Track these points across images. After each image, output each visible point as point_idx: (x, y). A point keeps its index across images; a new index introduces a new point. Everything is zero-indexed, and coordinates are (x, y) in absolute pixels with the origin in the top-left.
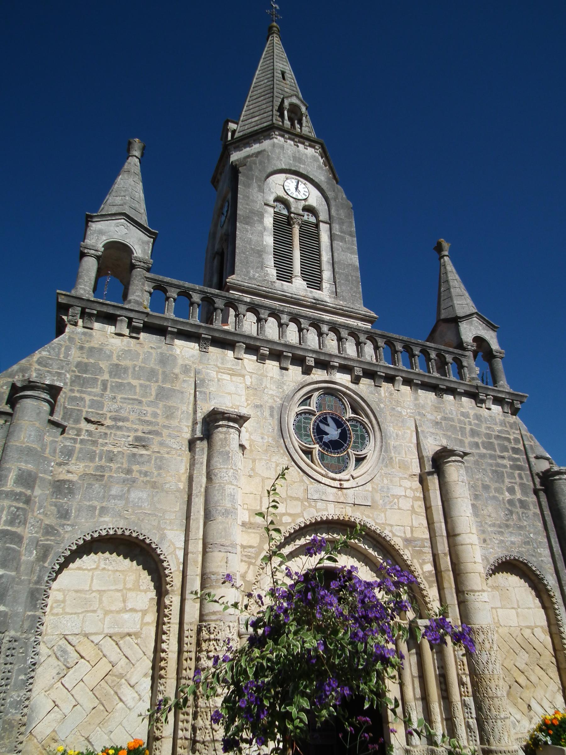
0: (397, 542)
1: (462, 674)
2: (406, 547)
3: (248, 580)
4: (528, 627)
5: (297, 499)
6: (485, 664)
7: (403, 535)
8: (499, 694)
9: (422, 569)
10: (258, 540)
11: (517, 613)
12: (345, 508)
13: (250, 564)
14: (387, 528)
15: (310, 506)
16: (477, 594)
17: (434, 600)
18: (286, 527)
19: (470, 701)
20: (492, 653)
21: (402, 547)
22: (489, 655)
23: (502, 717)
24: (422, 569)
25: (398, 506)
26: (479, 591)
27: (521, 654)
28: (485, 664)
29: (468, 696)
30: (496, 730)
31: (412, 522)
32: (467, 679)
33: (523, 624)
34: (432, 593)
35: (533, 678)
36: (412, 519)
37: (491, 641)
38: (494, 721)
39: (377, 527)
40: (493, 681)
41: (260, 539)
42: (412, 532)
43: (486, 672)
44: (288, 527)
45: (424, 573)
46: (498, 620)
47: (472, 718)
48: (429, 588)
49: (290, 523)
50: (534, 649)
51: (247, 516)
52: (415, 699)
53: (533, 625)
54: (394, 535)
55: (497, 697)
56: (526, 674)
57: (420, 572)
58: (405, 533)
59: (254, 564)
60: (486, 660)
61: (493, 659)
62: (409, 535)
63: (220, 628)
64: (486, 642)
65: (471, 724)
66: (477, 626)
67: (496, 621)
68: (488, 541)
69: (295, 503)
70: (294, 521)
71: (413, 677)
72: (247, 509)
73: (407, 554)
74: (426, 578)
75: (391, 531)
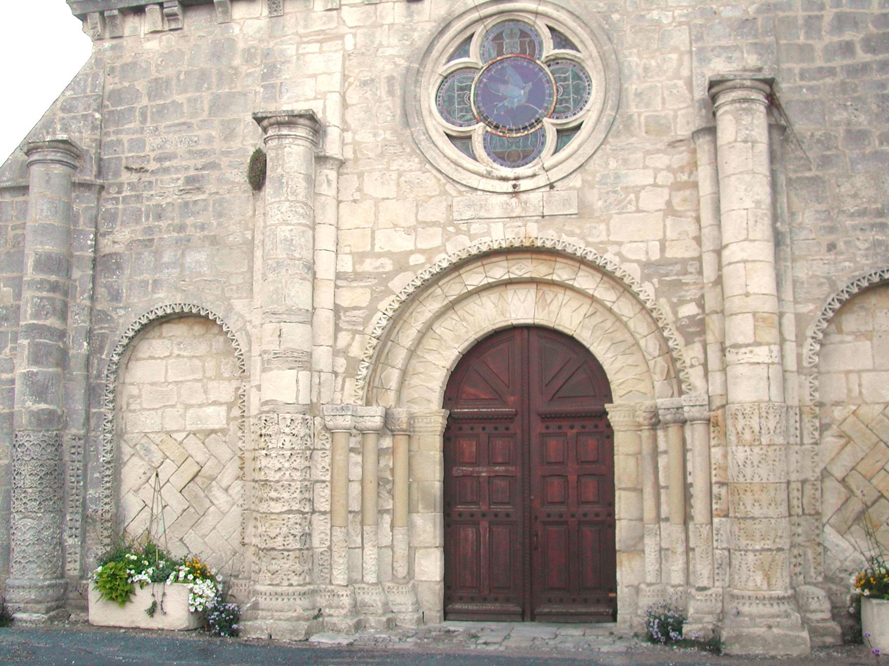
0: (632, 272)
2: (646, 278)
5: (435, 224)
6: (742, 466)
7: (643, 258)
9: (675, 313)
10: (368, 297)
12: (525, 225)
14: (609, 248)
15: (459, 232)
16: (743, 350)
17: (692, 366)
18: (415, 273)
22: (749, 452)
24: (675, 313)
25: (637, 206)
26: (747, 345)
28: (742, 466)
31: (664, 232)
36: (665, 226)
37: (757, 429)
39: (589, 249)
41: (372, 294)
42: (663, 249)
44: (420, 271)
45: (677, 319)
46: (860, 392)
49: (423, 265)
51: (350, 263)
54: (624, 259)
58: (647, 253)
59: (362, 333)
62: (655, 256)
67: (856, 392)
68: (841, 246)
69: (431, 230)
70: (429, 260)
72: (350, 253)
74: (681, 329)
75: (619, 254)
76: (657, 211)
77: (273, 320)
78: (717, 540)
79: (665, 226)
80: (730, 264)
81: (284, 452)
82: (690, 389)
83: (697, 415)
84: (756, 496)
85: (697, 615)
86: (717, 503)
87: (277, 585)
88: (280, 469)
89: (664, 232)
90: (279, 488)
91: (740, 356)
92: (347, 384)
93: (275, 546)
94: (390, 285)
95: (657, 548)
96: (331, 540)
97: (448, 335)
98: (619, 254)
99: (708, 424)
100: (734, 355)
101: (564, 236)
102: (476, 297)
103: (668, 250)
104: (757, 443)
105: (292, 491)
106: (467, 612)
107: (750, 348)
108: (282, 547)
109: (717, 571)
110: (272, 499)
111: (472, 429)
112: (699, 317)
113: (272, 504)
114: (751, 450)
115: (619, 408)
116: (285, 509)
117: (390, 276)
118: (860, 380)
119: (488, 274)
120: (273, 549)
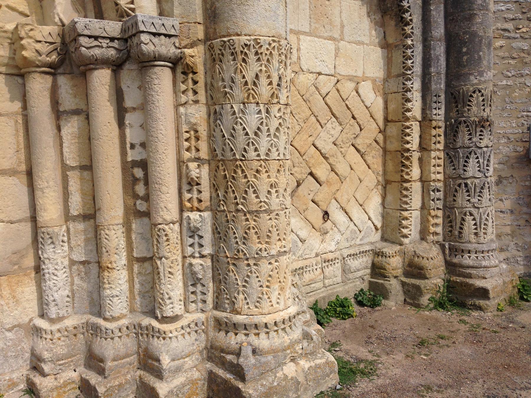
4: (351, 78)
6: (252, 135)
8: (275, 202)
11: (337, 50)
19: (202, 220)
20: (274, 110)
22: (264, 115)
23: (273, 252)
27: (329, 125)
28: (252, 135)
29: (199, 210)
30: (254, 281)
32: (202, 173)
33: (343, 70)
35: (342, 168)
37: (275, 80)
38: (251, 262)
40: (264, 176)
43: (252, 154)
46: (299, 58)
47: (202, 256)
50: (354, 117)
52: (68, 217)
53: (360, 74)
55: (269, 212)
56: (331, 160)
60: (255, 128)
61: (274, 124)
64: (263, 81)
65: (197, 268)
66: (244, 39)
71: (65, 168)
78: (191, 245)
83: (163, 51)
84: (273, 180)
85: (177, 362)
86: (189, 191)
95: (66, 262)
99: (173, 70)
104: (275, 101)
109: (191, 289)
114: (268, 112)
118: (299, 44)
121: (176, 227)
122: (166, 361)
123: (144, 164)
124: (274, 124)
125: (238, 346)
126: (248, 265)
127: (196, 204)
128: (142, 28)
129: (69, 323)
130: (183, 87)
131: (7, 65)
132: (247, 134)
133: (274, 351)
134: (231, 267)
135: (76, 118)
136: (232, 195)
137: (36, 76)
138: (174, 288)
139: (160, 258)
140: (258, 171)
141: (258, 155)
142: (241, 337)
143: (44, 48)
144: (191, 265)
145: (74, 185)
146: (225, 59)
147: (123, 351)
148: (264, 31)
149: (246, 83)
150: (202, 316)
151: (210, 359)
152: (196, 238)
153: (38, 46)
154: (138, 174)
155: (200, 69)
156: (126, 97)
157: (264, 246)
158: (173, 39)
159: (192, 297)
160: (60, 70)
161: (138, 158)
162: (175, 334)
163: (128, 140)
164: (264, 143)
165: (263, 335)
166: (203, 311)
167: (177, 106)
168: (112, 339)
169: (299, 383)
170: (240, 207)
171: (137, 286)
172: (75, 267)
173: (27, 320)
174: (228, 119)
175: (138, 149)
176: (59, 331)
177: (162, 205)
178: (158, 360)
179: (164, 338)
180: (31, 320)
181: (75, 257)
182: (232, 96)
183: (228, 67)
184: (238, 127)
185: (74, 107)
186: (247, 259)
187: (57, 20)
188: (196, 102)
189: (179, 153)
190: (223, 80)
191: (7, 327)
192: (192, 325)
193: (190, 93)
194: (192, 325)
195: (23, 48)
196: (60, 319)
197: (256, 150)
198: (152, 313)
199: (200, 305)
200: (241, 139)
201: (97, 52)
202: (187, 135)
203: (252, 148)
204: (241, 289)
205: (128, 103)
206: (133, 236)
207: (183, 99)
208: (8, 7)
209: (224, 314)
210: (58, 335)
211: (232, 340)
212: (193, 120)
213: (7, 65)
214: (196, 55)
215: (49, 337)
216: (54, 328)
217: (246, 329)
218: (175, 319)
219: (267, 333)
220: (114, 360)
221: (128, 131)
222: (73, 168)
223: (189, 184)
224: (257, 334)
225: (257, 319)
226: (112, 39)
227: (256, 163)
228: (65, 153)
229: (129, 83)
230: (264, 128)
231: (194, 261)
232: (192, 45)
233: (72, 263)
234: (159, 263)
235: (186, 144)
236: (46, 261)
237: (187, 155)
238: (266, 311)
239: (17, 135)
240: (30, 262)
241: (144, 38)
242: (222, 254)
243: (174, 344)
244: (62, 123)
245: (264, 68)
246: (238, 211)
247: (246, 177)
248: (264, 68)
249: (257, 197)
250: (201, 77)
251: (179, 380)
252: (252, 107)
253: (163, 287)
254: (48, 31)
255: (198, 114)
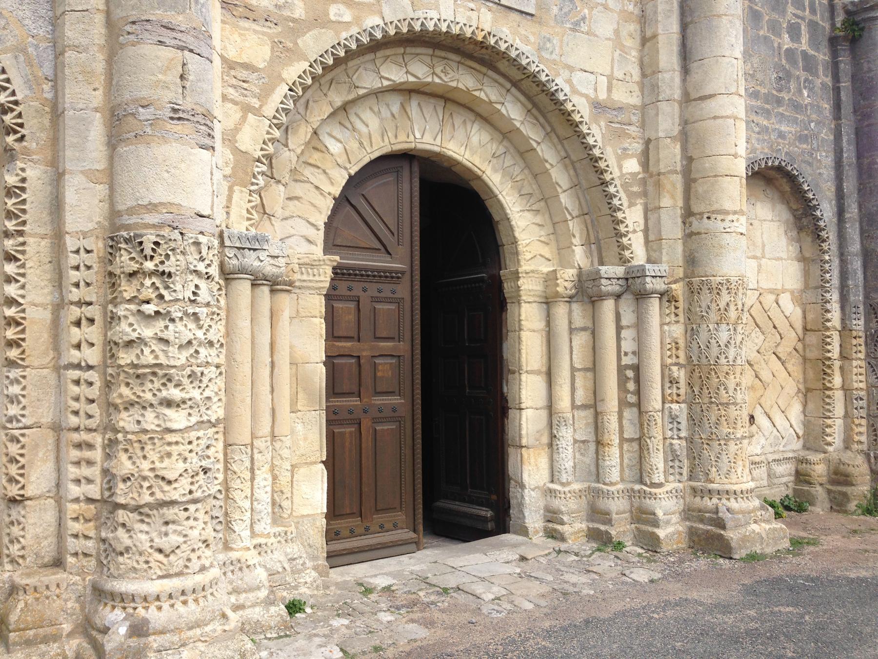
1: (672, 364)
2: (595, 119)
3: (243, 148)
4: (771, 291)
6: (723, 347)
9: (620, 167)
11: (760, 266)
12: (479, 10)
13: (247, 109)
14: (561, 72)
16: (730, 217)
17: (635, 231)
18: (337, 33)
19: (680, 409)
20: (739, 328)
21: (586, 119)
23: (739, 436)
25: (589, 27)
26: (735, 213)
27: (753, 335)
30: (724, 457)
31: (612, 68)
32: (680, 374)
33: (765, 285)
34: (633, 217)
35: (765, 375)
37: (740, 307)
38: (722, 442)
39: (542, 67)
42: (610, 89)
43: (723, 361)
44: (344, 35)
45: (622, 175)
47: (680, 438)
48: (629, 207)
50: (775, 327)
52: (574, 406)
53: (779, 287)
54: (575, 91)
55: (735, 404)
56: (755, 367)
57: (616, 174)
58: (596, 90)
59: (257, 112)
61: (739, 338)
62: (602, 96)
63: (173, 244)
64: (732, 307)
65: (677, 447)
66: (719, 279)
70: (357, 20)
71: (573, 369)
73: (596, 133)
74: (625, 186)
75: (569, 81)
76: (606, 39)
77: (167, 41)
79: (613, 59)
80: (715, 118)
81: (197, 310)
82: (632, 258)
84: (738, 380)
85: (666, 517)
87: (179, 574)
88: (190, 343)
89: (612, 68)
90: (185, 381)
91: (727, 224)
92: (236, 197)
93: (175, 496)
94: (299, 41)
96: (226, 469)
97: (335, 147)
98: (569, 81)
100: (720, 222)
101: (518, 41)
102: (372, 101)
103: (614, 90)
105: (203, 385)
106: (351, 552)
107: (737, 216)
108: (189, 497)
109: (671, 464)
110: (169, 403)
111: (350, 289)
112: (640, 176)
113: (170, 412)
114: (735, 330)
115: (531, 275)
116: (194, 420)
117: (297, 28)
119: (410, 69)
120: (173, 503)
121: (660, 414)
122: (660, 513)
123: (637, 368)
124: (739, 338)
125: (714, 506)
126: (720, 444)
127: (675, 398)
128: (648, 274)
129: (576, 486)
130: (668, 311)
131: (540, 296)
132: (719, 346)
133: (742, 512)
134: (705, 446)
135: (583, 333)
136: (707, 392)
137: (561, 304)
138: (657, 460)
139: (650, 438)
140: (727, 373)
141: (728, 362)
142: (715, 501)
143: (569, 285)
144: (671, 444)
145: (579, 383)
146: (702, 293)
147: (622, 508)
148: (733, 273)
149: (719, 309)
150: (681, 486)
151: (687, 519)
152: (675, 423)
153: (566, 284)
154: (634, 375)
155: (681, 299)
156: (622, 318)
157: (732, 431)
158: (664, 279)
159: (671, 471)
160: (574, 299)
161: (630, 363)
162: (663, 496)
163: (623, 349)
164: (732, 353)
165: (732, 500)
166: (680, 481)
167: (662, 325)
168: (613, 498)
169: (763, 538)
170: (713, 400)
171: (626, 461)
172: (577, 445)
173: (542, 484)
174: (703, 336)
175: (630, 356)
176: (569, 492)
177: (653, 397)
178: (654, 514)
179: (655, 499)
180: (545, 484)
181: (578, 438)
182: (708, 319)
183: (706, 298)
184: (713, 341)
185: (582, 325)
186: (719, 440)
187: (576, 265)
188: (677, 322)
189: (662, 358)
190: (700, 307)
191: (532, 487)
192: (674, 491)
193: (673, 316)
194: (674, 491)
195: (557, 285)
196: (568, 483)
197: (726, 357)
198: (641, 481)
199: (678, 477)
200: (715, 351)
201: (610, 288)
202: (669, 346)
203: (724, 356)
204: (714, 463)
205: (624, 322)
206: (624, 422)
207: (668, 320)
208: (541, 255)
209: (699, 484)
210: (569, 495)
211: (709, 503)
212: (675, 335)
213: (540, 296)
214: (678, 289)
215: (563, 496)
216: (567, 489)
217: (719, 494)
218: (660, 485)
219: (736, 499)
220: (617, 514)
221: (623, 343)
222: (579, 370)
223: (671, 382)
224: (728, 499)
225: (727, 487)
226: (618, 279)
227: (726, 367)
228: (574, 359)
229: (625, 308)
230: (732, 342)
231: (674, 442)
232: (675, 282)
233: (575, 441)
234: (648, 441)
235: (669, 353)
236: (561, 439)
237: (669, 361)
238: (733, 481)
239: (542, 346)
240: (545, 439)
241: (648, 279)
242: (698, 436)
243: (664, 503)
244: (573, 337)
245: (732, 299)
246: (712, 403)
247: (718, 377)
248: (732, 299)
249: (727, 393)
250: (681, 304)
251: (670, 529)
252: (723, 327)
253: (652, 460)
254: (570, 273)
255: (677, 331)
